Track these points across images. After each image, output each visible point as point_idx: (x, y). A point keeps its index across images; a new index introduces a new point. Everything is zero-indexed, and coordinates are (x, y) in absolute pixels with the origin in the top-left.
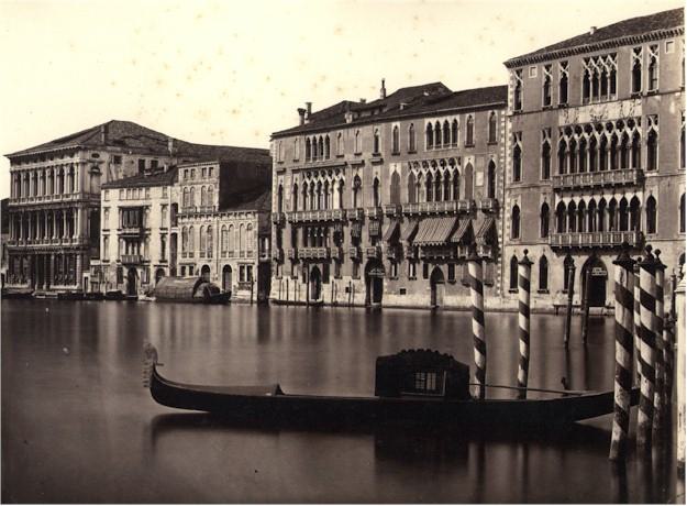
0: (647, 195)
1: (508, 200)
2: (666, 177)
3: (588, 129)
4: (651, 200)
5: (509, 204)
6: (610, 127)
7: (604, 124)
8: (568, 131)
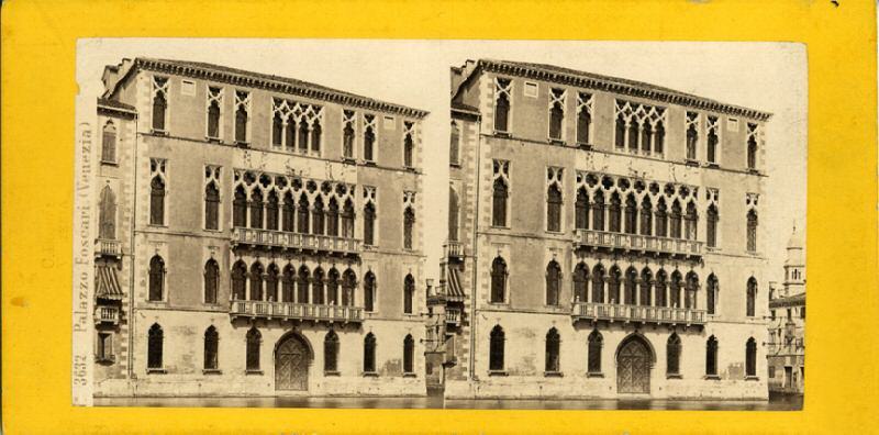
0: (365, 271)
1: (138, 249)
2: (388, 254)
3: (281, 181)
4: (370, 277)
5: (144, 253)
6: (312, 186)
7: (305, 182)
8: (250, 177)
